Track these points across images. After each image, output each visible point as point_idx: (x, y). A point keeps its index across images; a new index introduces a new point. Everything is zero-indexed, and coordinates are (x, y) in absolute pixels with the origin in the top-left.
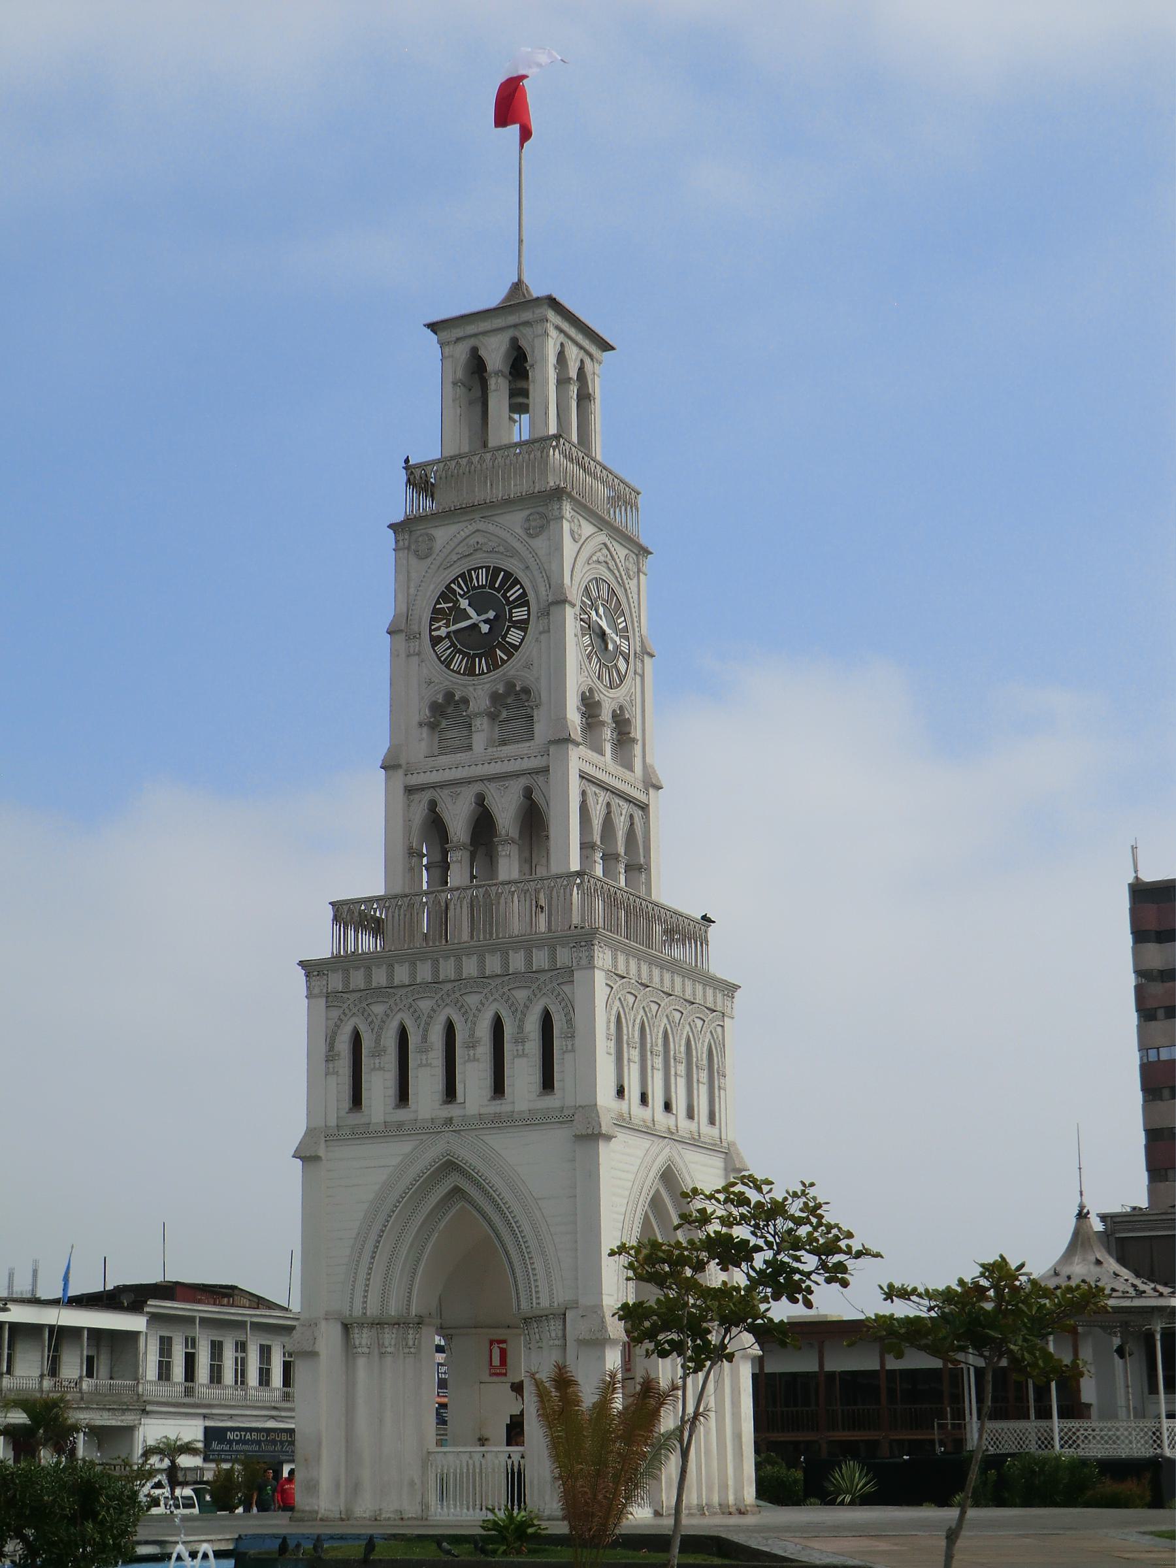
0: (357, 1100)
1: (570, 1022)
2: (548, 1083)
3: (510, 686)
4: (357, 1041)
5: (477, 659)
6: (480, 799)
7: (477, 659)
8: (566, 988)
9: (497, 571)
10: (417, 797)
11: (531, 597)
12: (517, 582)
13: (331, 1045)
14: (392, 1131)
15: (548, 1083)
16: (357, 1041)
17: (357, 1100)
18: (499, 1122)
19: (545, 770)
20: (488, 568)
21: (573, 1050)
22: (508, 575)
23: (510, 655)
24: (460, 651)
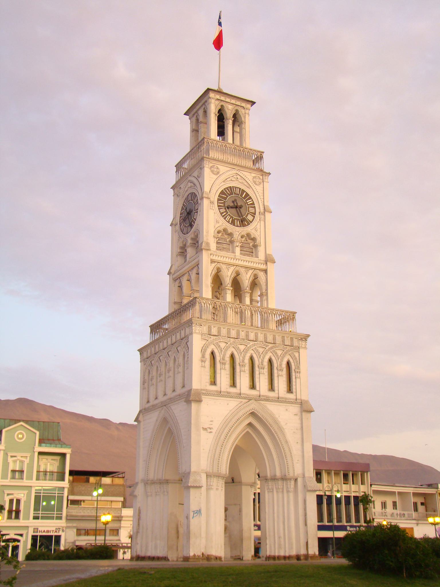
1: (299, 368)
3: (248, 235)
5: (236, 220)
6: (238, 274)
7: (236, 220)
9: (243, 191)
10: (214, 265)
11: (256, 205)
12: (250, 198)
13: (203, 356)
14: (228, 395)
15: (290, 390)
19: (266, 271)
20: (240, 189)
22: (247, 195)
23: (249, 224)
24: (229, 215)
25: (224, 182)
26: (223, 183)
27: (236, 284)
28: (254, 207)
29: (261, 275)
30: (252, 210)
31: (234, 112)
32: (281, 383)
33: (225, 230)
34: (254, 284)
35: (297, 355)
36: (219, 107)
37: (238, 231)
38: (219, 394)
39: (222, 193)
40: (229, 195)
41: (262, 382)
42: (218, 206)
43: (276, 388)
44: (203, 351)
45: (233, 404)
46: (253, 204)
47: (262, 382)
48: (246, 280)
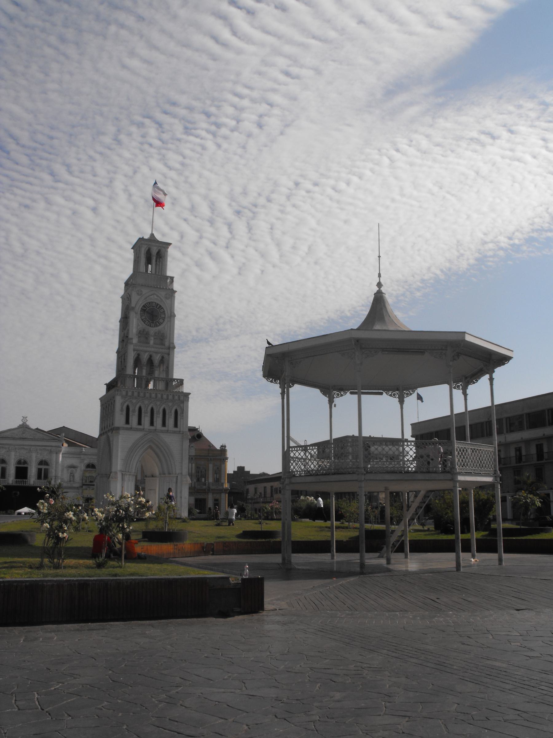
0: (127, 422)
2: (176, 425)
4: (128, 408)
6: (151, 356)
8: (182, 405)
9: (158, 304)
10: (135, 352)
11: (166, 313)
13: (122, 408)
14: (137, 430)
15: (176, 425)
16: (128, 408)
17: (127, 422)
18: (162, 432)
20: (156, 303)
21: (183, 418)
22: (160, 306)
23: (160, 325)
24: (148, 320)
25: (145, 299)
26: (144, 300)
27: (150, 361)
28: (165, 314)
29: (166, 356)
30: (163, 316)
31: (157, 251)
32: (170, 421)
33: (144, 330)
34: (162, 361)
35: (182, 405)
36: (147, 249)
37: (153, 330)
38: (131, 429)
39: (144, 306)
40: (148, 307)
41: (158, 421)
42: (140, 315)
43: (167, 425)
44: (122, 405)
45: (138, 435)
46: (164, 312)
47: (158, 421)
48: (157, 359)
